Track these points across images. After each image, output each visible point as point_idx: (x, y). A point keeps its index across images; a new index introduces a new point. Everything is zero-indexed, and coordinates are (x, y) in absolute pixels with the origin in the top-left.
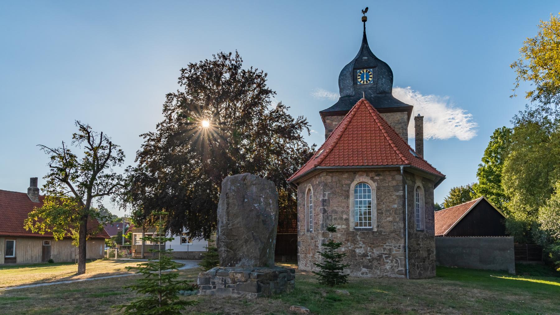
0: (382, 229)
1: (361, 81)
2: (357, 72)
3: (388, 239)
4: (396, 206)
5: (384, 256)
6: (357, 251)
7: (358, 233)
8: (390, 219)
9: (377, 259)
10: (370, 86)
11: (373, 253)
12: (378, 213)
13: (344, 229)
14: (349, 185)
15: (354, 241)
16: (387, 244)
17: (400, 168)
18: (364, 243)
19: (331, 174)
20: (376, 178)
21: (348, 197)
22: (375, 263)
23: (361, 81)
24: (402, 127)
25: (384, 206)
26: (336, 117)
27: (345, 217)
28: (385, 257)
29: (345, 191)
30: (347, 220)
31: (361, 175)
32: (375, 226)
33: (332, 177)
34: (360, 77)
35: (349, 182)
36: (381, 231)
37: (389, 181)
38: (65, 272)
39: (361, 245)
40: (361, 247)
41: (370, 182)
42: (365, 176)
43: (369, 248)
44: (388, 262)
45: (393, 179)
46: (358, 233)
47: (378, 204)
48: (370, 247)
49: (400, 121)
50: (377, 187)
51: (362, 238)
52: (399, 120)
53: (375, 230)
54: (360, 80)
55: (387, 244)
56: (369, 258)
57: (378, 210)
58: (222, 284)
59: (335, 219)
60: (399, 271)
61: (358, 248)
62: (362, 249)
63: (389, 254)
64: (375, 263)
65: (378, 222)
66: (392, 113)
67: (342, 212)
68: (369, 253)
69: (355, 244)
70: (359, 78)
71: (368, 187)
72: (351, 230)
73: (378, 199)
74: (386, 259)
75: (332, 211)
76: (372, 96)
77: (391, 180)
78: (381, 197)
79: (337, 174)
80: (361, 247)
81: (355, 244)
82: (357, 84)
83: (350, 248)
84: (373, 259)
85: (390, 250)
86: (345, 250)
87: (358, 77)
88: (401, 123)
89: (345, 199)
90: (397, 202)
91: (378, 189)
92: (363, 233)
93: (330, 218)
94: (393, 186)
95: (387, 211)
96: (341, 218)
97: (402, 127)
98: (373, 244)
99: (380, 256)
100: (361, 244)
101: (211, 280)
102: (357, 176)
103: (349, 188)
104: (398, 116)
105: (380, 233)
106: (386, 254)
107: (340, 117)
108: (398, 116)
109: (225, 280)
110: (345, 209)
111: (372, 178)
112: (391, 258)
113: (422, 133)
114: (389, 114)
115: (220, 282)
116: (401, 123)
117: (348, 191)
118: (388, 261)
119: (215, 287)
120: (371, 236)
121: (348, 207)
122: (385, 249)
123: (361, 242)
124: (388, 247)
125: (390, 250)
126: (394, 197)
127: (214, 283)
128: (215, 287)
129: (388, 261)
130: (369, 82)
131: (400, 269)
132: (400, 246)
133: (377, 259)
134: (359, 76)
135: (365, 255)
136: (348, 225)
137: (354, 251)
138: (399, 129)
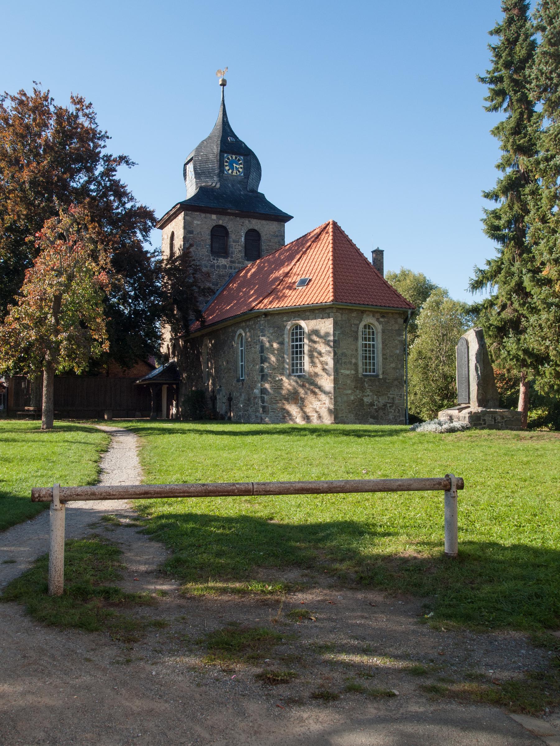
0: (386, 376)
1: (229, 170)
2: (224, 156)
3: (391, 387)
4: (398, 352)
5: (388, 405)
6: (365, 399)
7: (366, 380)
8: (393, 365)
9: (382, 409)
10: (239, 178)
11: (379, 402)
12: (384, 359)
13: (353, 374)
14: (357, 325)
15: (362, 389)
16: (391, 392)
17: (407, 312)
18: (371, 391)
19: (340, 311)
20: (382, 320)
21: (356, 339)
22: (381, 413)
23: (229, 170)
24: (279, 242)
25: (388, 351)
26: (198, 213)
27: (354, 361)
28: (390, 406)
29: (354, 332)
30: (356, 364)
31: (368, 315)
32: (380, 372)
33: (342, 314)
34: (227, 164)
35: (358, 322)
36: (386, 378)
37: (393, 325)
38: (141, 424)
39: (368, 393)
40: (368, 396)
41: (376, 323)
42: (371, 316)
43: (375, 397)
44: (391, 412)
45: (396, 322)
46: (366, 380)
47: (383, 349)
48: (376, 395)
49: (277, 233)
50: (382, 329)
51: (369, 386)
52: (275, 232)
53: (381, 377)
54: (227, 168)
55: (391, 392)
56: (375, 407)
57: (383, 355)
58: (491, 420)
59: (345, 363)
60: (400, 421)
61: (366, 396)
62: (370, 397)
63: (393, 403)
64: (381, 413)
65: (383, 368)
66: (267, 222)
67: (352, 355)
68: (376, 402)
69: (363, 392)
70: (226, 166)
71: (372, 329)
72: (360, 376)
73: (383, 343)
74: (390, 409)
75: (342, 354)
76: (242, 193)
77: (394, 323)
78: (385, 341)
79: (347, 312)
80: (368, 396)
81: (363, 392)
82: (223, 173)
83: (358, 396)
84: (379, 409)
85: (393, 398)
86: (355, 399)
87: (225, 164)
88: (277, 236)
89: (354, 340)
90: (399, 347)
91: (383, 332)
92: (370, 380)
93: (340, 362)
94: (396, 330)
95: (391, 356)
96: (350, 363)
97: (279, 242)
98: (379, 392)
99: (385, 405)
100: (368, 392)
101: (482, 418)
102: (365, 316)
103: (358, 328)
104: (274, 226)
105: (384, 379)
106: (390, 403)
107: (203, 215)
108: (274, 226)
109: (495, 418)
110: (354, 352)
111: (378, 320)
112: (394, 408)
113: (383, 269)
114: (264, 222)
115: (490, 418)
116: (277, 236)
117: (357, 332)
118: (391, 410)
119: (485, 424)
120: (377, 383)
121: (357, 350)
122: (389, 397)
123: (368, 390)
124: (391, 396)
125: (393, 398)
126: (396, 341)
127: (484, 420)
128: (485, 424)
129: (391, 410)
130: (238, 173)
131: (401, 419)
132: (401, 395)
133: (382, 409)
134: (227, 162)
135: (372, 404)
136: (357, 370)
137: (362, 400)
138: (276, 243)
